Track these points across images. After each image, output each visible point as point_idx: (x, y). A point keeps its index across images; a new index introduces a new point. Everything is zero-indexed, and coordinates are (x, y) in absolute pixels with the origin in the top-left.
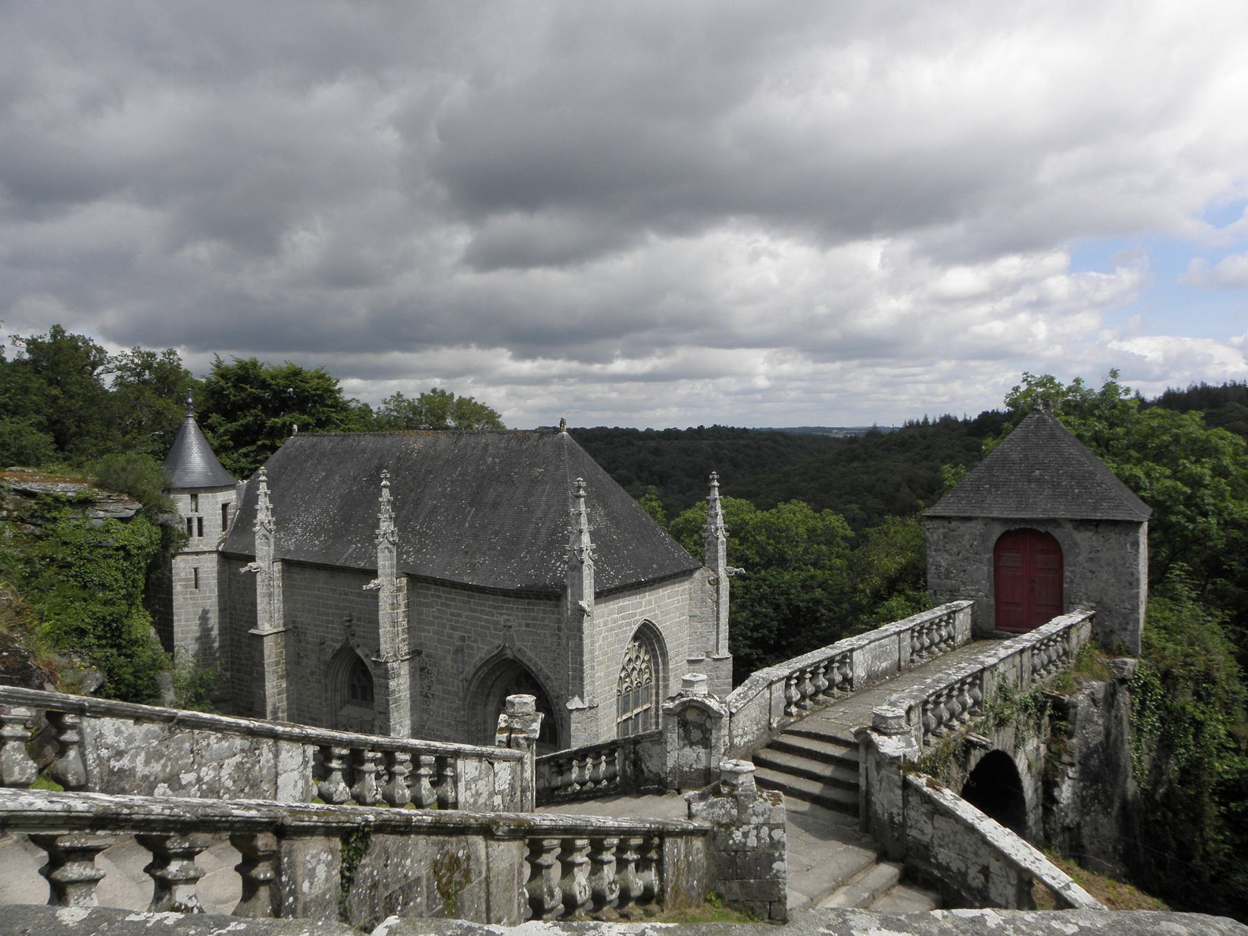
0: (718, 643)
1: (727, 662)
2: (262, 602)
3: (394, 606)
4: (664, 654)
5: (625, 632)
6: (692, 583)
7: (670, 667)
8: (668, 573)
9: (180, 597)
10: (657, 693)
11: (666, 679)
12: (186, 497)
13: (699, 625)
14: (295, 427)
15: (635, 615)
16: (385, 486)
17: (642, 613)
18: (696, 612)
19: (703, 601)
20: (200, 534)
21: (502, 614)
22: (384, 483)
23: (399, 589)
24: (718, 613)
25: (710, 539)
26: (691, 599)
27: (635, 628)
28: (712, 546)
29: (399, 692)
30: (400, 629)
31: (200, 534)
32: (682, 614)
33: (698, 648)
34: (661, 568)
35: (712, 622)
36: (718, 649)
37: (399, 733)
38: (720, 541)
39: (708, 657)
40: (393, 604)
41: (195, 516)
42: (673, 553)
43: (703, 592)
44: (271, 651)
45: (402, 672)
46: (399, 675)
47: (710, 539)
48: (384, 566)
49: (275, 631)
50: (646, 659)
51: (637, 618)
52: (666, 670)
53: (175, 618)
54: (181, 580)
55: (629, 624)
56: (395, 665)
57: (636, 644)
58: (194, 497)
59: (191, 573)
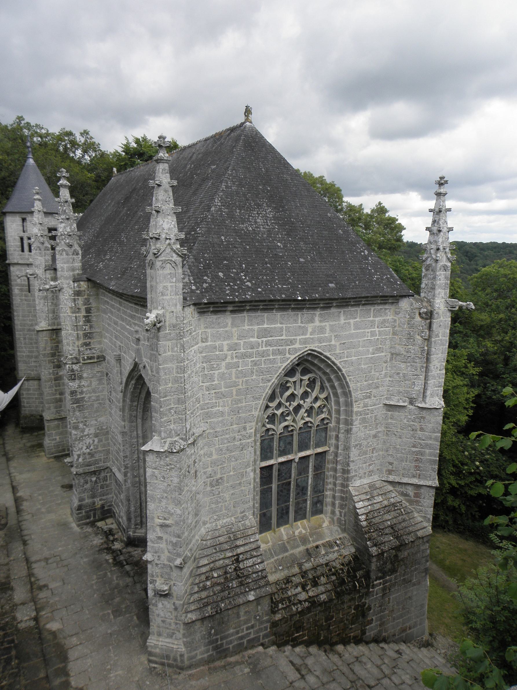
0: (425, 389)
1: (436, 413)
2: (40, 303)
3: (76, 310)
4: (347, 394)
5: (273, 361)
6: (397, 313)
7: (355, 409)
8: (349, 295)
9: (18, 298)
10: (337, 437)
11: (348, 423)
12: (18, 219)
13: (403, 366)
14: (115, 169)
15: (292, 342)
16: (65, 186)
17: (305, 342)
18: (400, 349)
19: (410, 337)
20: (30, 251)
21: (135, 324)
22: (63, 182)
23: (78, 293)
24: (428, 353)
25: (428, 262)
26: (394, 333)
27: (292, 358)
28: (430, 272)
29: (82, 393)
30: (81, 333)
31: (30, 251)
32: (380, 350)
33: (399, 392)
34: (341, 287)
35: (419, 363)
36: (424, 397)
37: (83, 431)
38: (440, 264)
39: (411, 403)
40: (71, 308)
41: (25, 236)
42: (371, 275)
43: (411, 326)
44: (46, 343)
45: (85, 375)
46: (81, 378)
47: (428, 262)
48: (62, 268)
49: (50, 328)
50: (322, 396)
51: (297, 346)
52: (349, 413)
53: (15, 314)
54: (17, 285)
55: (280, 352)
56: (75, 367)
57: (306, 377)
58: (24, 220)
59: (24, 280)
